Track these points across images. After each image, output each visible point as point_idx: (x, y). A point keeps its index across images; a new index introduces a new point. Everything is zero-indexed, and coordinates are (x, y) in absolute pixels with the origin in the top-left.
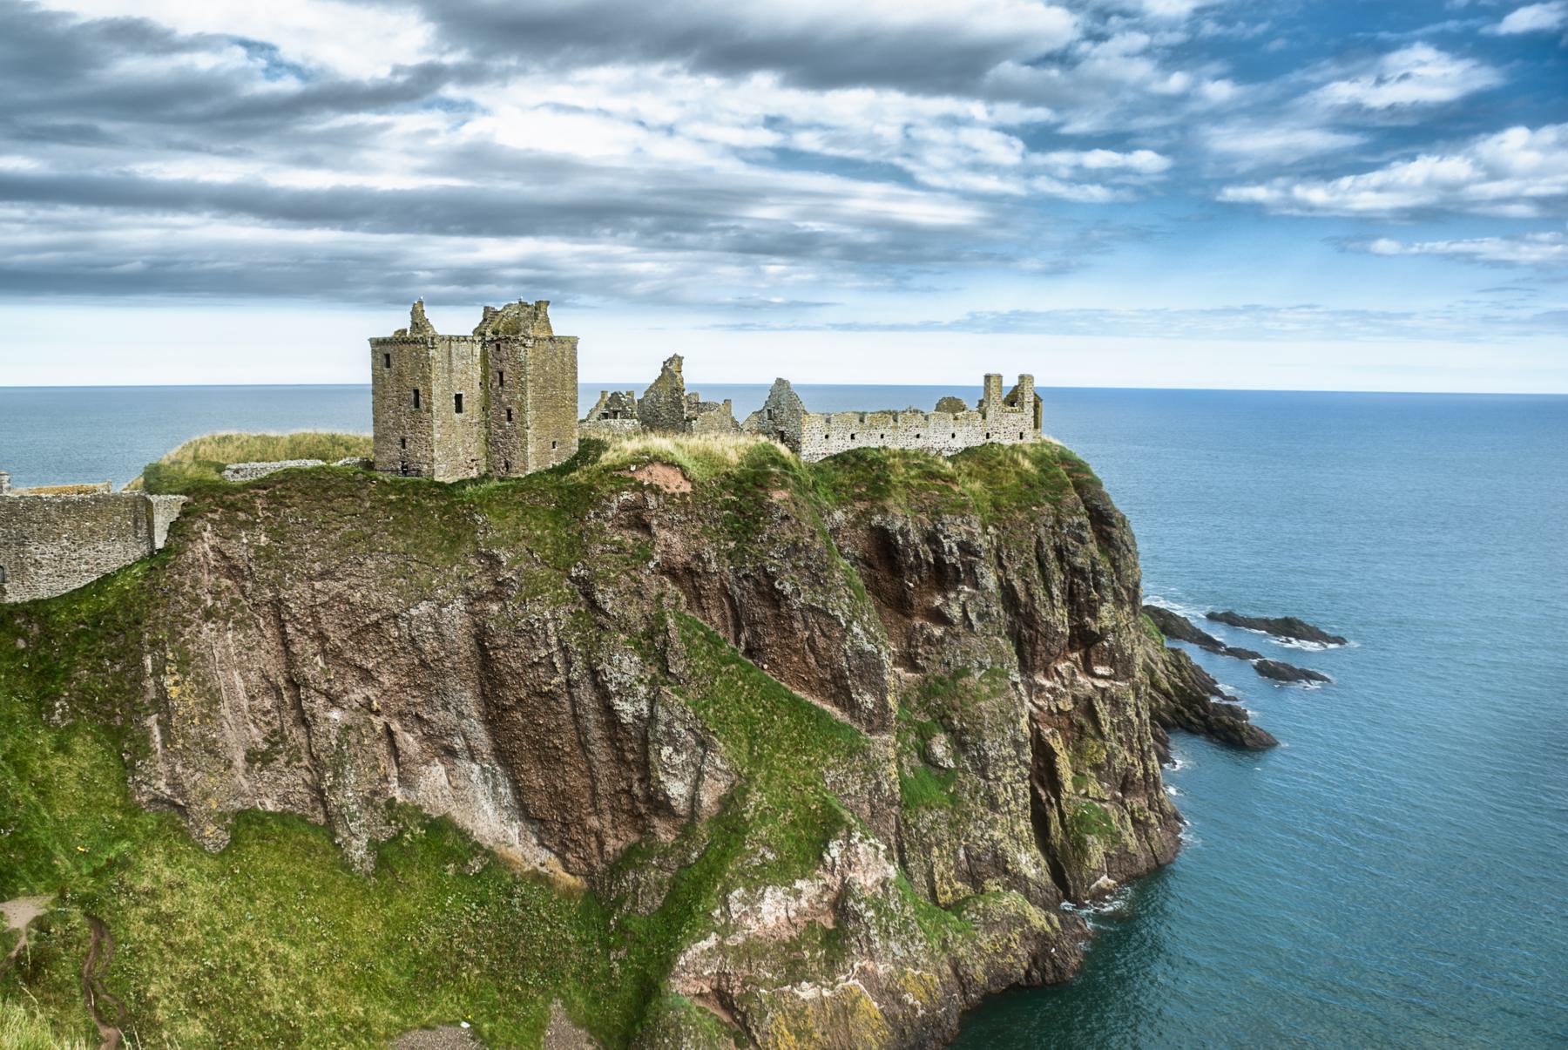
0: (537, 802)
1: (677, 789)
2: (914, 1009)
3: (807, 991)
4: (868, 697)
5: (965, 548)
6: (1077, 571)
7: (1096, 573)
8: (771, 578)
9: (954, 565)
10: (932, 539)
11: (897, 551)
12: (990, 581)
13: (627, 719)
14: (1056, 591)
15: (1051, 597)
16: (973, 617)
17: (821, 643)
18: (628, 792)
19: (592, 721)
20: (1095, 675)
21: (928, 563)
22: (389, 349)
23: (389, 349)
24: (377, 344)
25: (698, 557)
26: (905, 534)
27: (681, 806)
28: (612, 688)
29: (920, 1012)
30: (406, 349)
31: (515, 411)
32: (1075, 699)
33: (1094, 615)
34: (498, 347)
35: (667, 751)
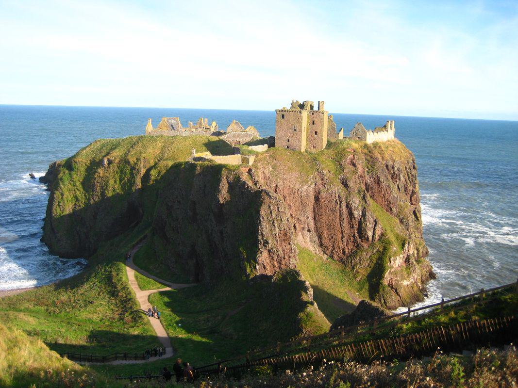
0: (326, 241)
1: (370, 234)
2: (420, 286)
3: (405, 283)
10: (393, 168)
12: (402, 179)
13: (357, 216)
17: (386, 194)
18: (354, 236)
19: (345, 215)
20: (412, 204)
22: (284, 113)
25: (364, 172)
27: (370, 239)
28: (353, 208)
29: (421, 288)
31: (318, 131)
33: (415, 188)
34: (313, 114)
35: (368, 224)
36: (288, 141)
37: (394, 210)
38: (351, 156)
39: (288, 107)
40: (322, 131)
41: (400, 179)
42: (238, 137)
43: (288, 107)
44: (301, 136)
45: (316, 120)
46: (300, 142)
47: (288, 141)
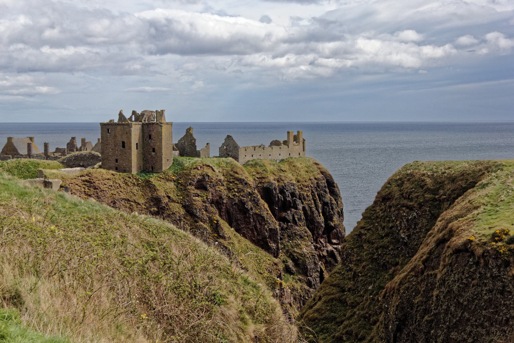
4: (273, 245)
5: (293, 195)
6: (325, 204)
7: (332, 204)
8: (243, 204)
9: (289, 201)
10: (282, 191)
11: (273, 195)
12: (300, 207)
14: (320, 211)
15: (319, 213)
16: (296, 219)
21: (281, 200)
23: (109, 127)
24: (103, 125)
25: (221, 197)
26: (275, 189)
30: (119, 128)
31: (156, 148)
32: (327, 251)
36: (117, 161)
37: (273, 245)
38: (199, 177)
39: (116, 121)
40: (161, 148)
41: (296, 208)
42: (81, 160)
43: (116, 121)
44: (130, 155)
45: (153, 134)
46: (130, 162)
47: (117, 161)
